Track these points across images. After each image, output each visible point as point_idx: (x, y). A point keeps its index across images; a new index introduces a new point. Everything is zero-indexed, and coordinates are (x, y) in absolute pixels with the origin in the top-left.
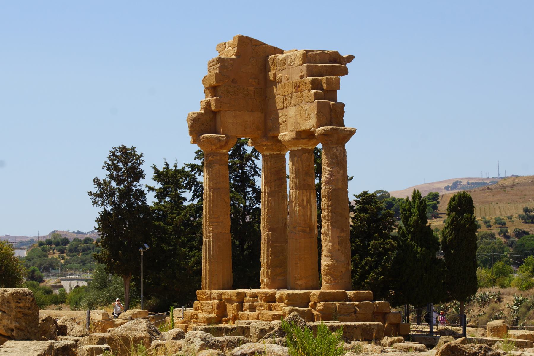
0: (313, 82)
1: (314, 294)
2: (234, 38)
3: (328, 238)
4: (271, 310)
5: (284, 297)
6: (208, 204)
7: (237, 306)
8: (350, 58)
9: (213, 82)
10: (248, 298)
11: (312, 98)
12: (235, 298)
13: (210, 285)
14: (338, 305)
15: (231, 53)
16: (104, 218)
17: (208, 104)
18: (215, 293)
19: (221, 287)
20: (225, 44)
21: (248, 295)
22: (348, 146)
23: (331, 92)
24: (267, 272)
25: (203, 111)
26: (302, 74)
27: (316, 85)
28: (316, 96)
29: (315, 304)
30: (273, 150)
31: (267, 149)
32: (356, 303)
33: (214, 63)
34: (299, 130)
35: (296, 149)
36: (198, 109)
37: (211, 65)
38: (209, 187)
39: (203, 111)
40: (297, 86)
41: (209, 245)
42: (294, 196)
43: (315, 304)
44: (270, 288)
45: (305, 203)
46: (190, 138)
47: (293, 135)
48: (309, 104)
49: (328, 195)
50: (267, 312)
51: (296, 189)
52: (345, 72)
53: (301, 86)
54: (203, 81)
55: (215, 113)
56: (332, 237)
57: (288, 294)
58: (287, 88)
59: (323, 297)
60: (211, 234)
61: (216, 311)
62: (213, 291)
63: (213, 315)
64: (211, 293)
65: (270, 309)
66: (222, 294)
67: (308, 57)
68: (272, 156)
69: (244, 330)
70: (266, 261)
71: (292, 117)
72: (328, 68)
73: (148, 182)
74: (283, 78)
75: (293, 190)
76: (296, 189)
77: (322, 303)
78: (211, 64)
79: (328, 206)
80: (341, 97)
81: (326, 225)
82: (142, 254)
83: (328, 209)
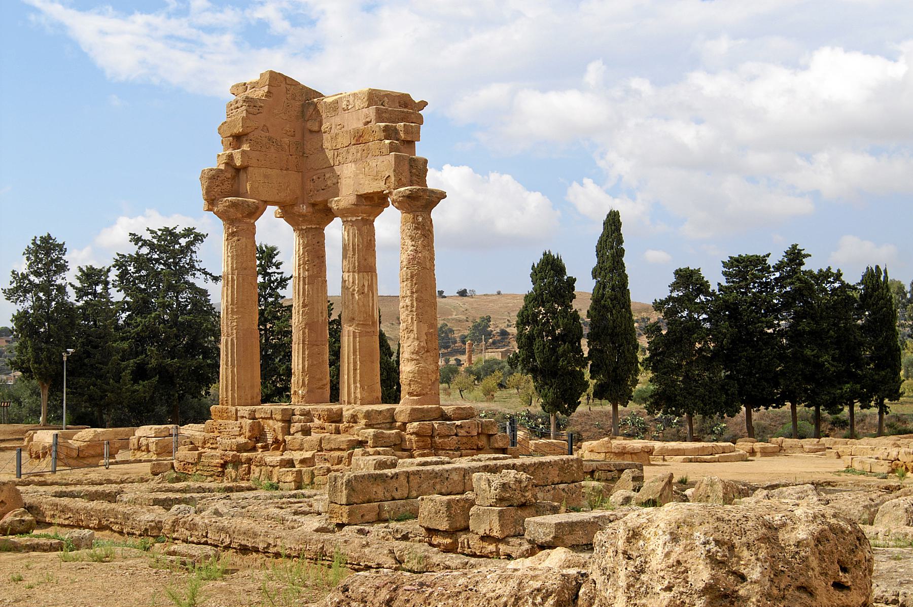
0: (386, 129)
1: (401, 411)
2: (262, 75)
3: (412, 336)
4: (339, 433)
5: (360, 416)
6: (230, 291)
7: (282, 427)
8: (424, 104)
9: (238, 129)
10: (296, 418)
11: (384, 151)
12: (279, 417)
13: (233, 398)
14: (436, 426)
15: (260, 93)
16: (21, 318)
17: (230, 157)
18: (244, 410)
19: (249, 401)
20: (245, 84)
21: (297, 413)
22: (435, 214)
23: (410, 143)
24: (303, 380)
25: (222, 167)
26: (368, 120)
27: (389, 133)
28: (392, 148)
29: (404, 424)
30: (311, 222)
31: (304, 221)
32: (458, 423)
33: (239, 105)
34: (362, 192)
35: (354, 219)
36: (216, 164)
37: (232, 107)
38: (232, 267)
39: (222, 167)
40: (359, 138)
41: (232, 344)
42: (351, 280)
43: (404, 424)
44: (308, 402)
45: (366, 290)
46: (202, 203)
47: (352, 199)
48: (381, 158)
49: (412, 277)
50: (334, 436)
51: (354, 272)
52: (420, 120)
53: (366, 137)
54: (219, 129)
55: (238, 170)
56: (419, 332)
57: (367, 411)
58: (340, 139)
59: (416, 415)
60: (235, 331)
61: (248, 434)
62: (239, 408)
63: (242, 440)
64: (236, 410)
65: (338, 432)
66: (255, 411)
67: (375, 97)
68: (308, 230)
69: (408, 477)
70: (301, 366)
71: (350, 177)
72: (398, 116)
73: (70, 278)
74: (333, 126)
75: (349, 272)
76: (354, 272)
77: (416, 424)
78: (233, 107)
79: (412, 293)
80: (421, 150)
81: (410, 318)
82: (65, 359)
83: (412, 296)
